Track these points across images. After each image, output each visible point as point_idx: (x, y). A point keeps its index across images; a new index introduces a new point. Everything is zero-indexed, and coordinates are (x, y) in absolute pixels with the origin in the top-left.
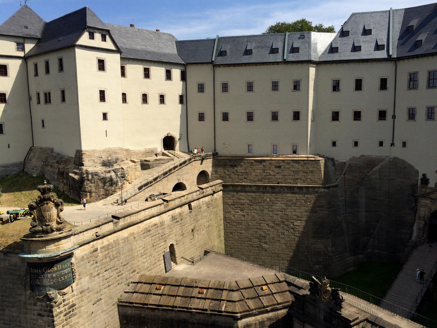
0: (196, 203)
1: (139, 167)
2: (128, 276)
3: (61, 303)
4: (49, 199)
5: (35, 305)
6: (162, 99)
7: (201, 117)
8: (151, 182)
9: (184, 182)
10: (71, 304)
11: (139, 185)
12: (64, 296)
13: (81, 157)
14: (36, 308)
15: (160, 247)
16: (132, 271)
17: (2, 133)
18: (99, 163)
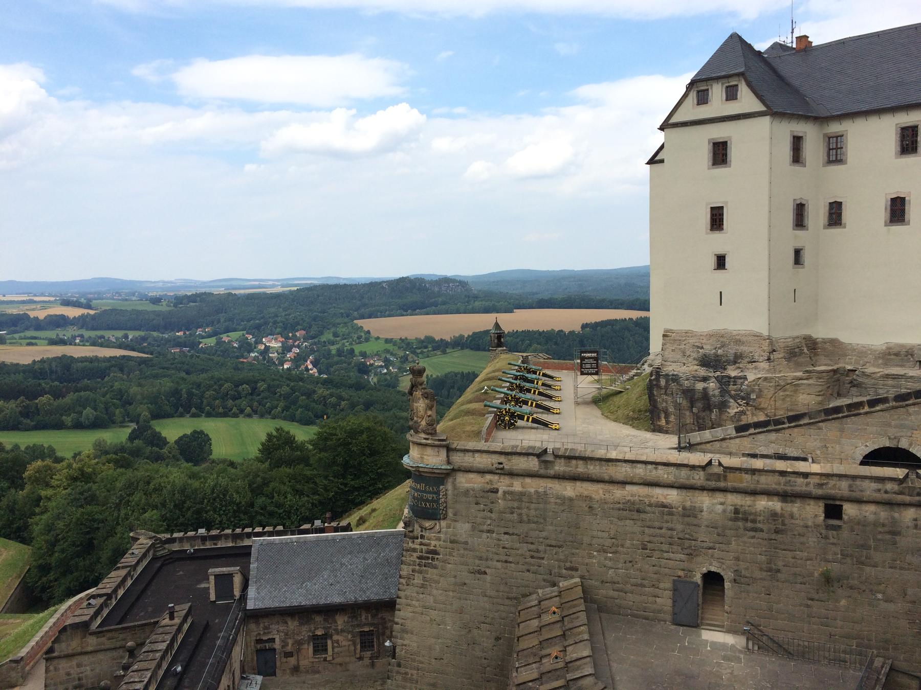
0: (875, 514)
2: (556, 571)
3: (417, 538)
8: (778, 422)
10: (432, 548)
12: (424, 530)
15: (667, 559)
16: (568, 565)
18: (694, 359)
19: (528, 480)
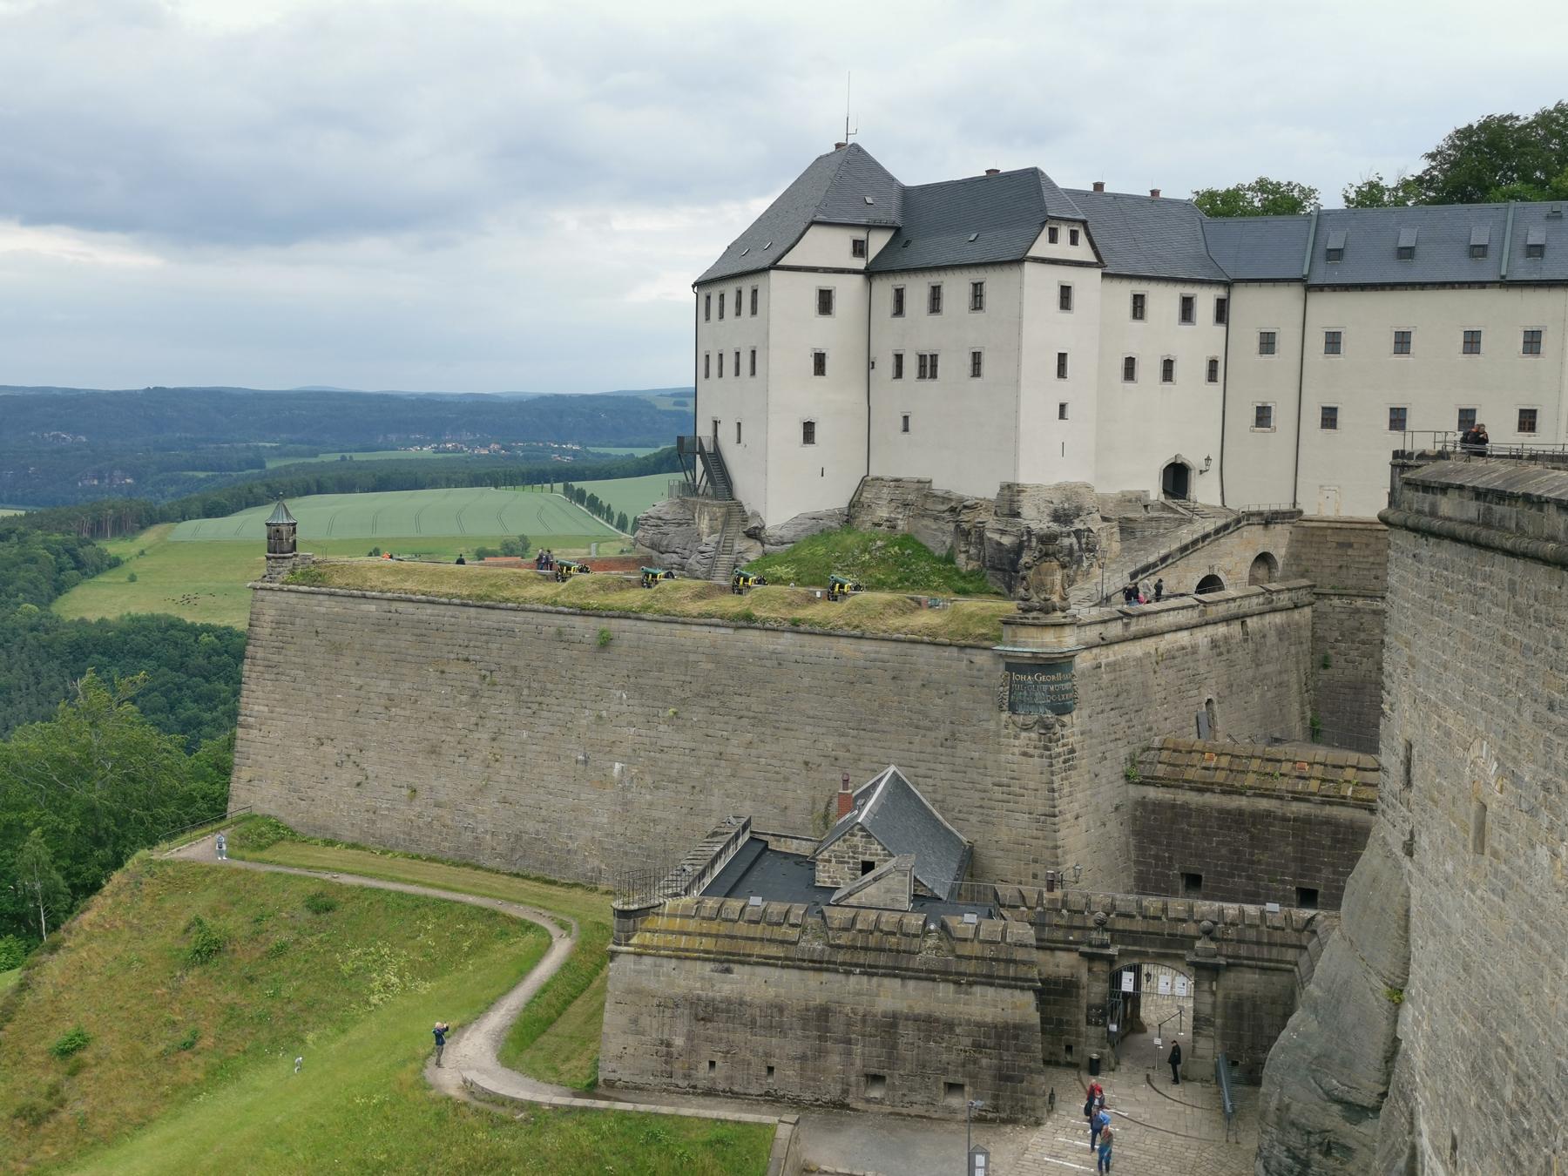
1: (1116, 530)
4: (1054, 554)
5: (1016, 737)
6: (1168, 368)
7: (1263, 416)
8: (1154, 565)
9: (1221, 575)
11: (1132, 569)
13: (1016, 498)
14: (1017, 743)
17: (813, 443)
19: (1116, 647)
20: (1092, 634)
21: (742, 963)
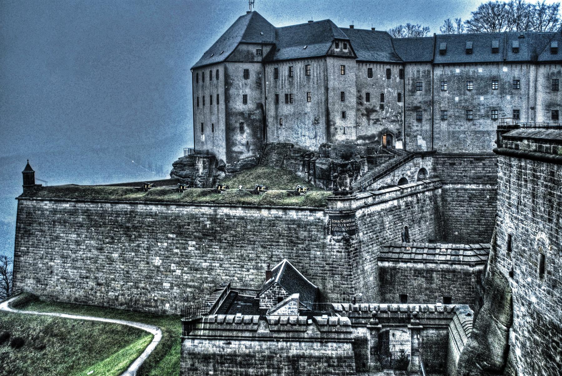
9: (407, 178)
20: (360, 203)
21: (235, 340)
